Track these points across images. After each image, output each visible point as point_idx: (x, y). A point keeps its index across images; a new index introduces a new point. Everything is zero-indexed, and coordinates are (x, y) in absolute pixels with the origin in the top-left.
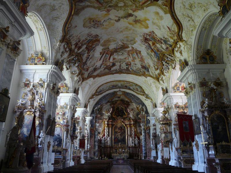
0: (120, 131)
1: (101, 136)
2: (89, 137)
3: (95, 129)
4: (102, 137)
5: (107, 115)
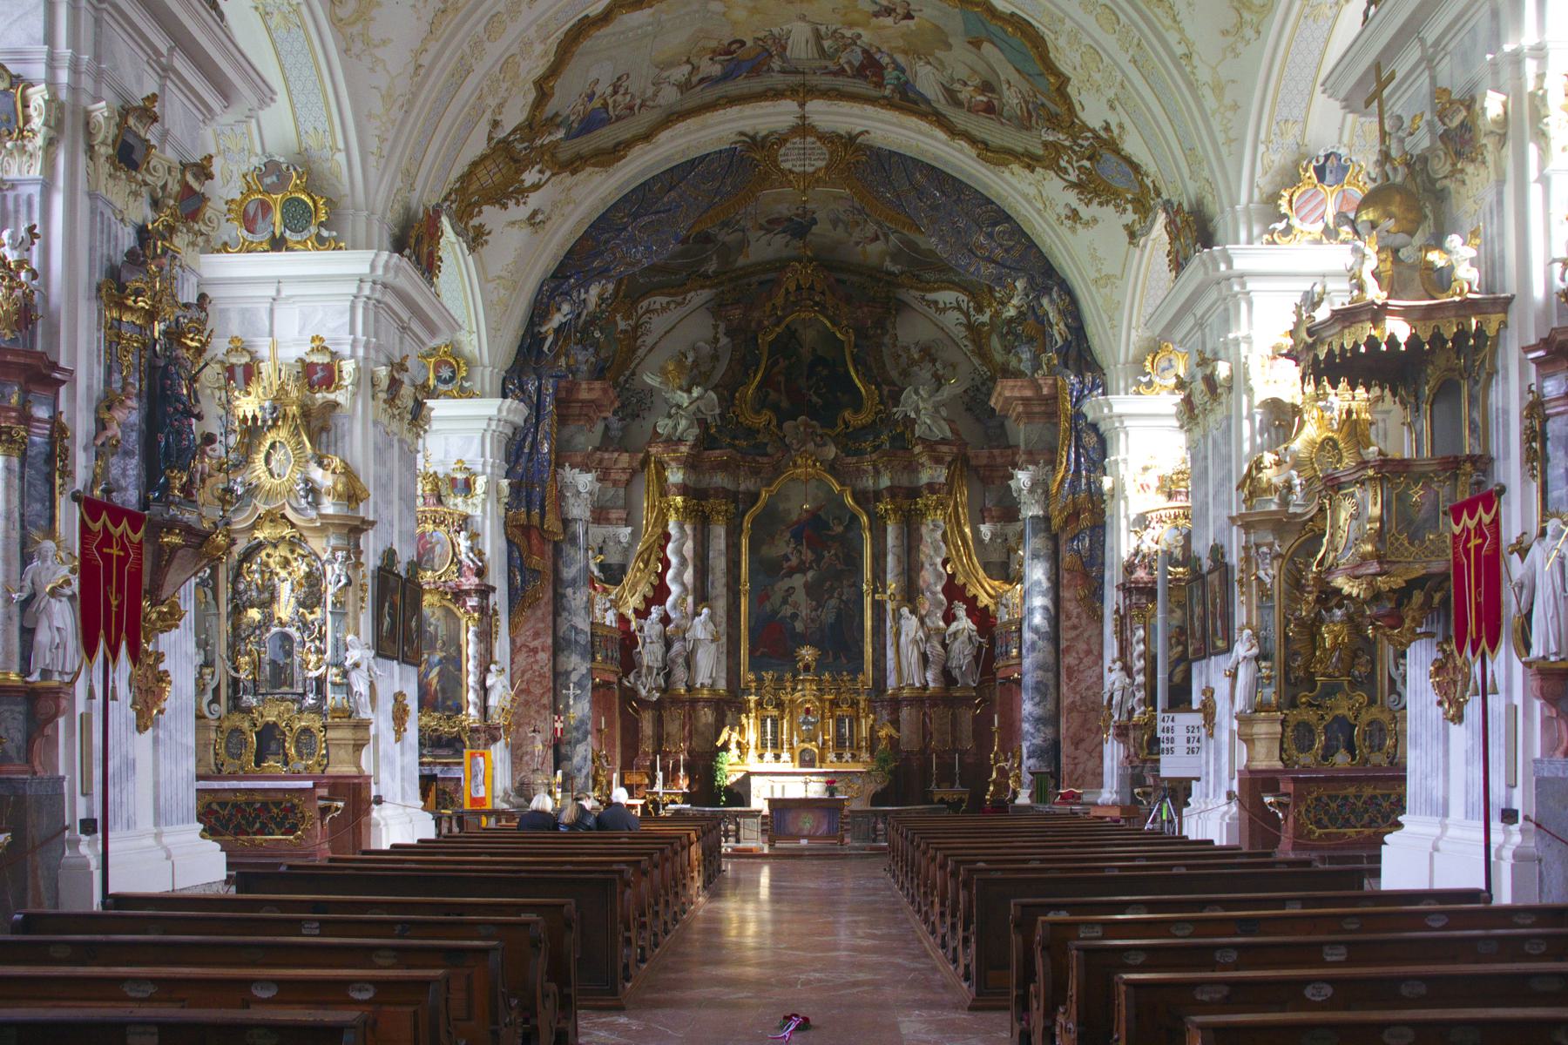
0: (808, 555)
1: (634, 601)
2: (499, 599)
3: (552, 523)
4: (643, 614)
5: (683, 398)
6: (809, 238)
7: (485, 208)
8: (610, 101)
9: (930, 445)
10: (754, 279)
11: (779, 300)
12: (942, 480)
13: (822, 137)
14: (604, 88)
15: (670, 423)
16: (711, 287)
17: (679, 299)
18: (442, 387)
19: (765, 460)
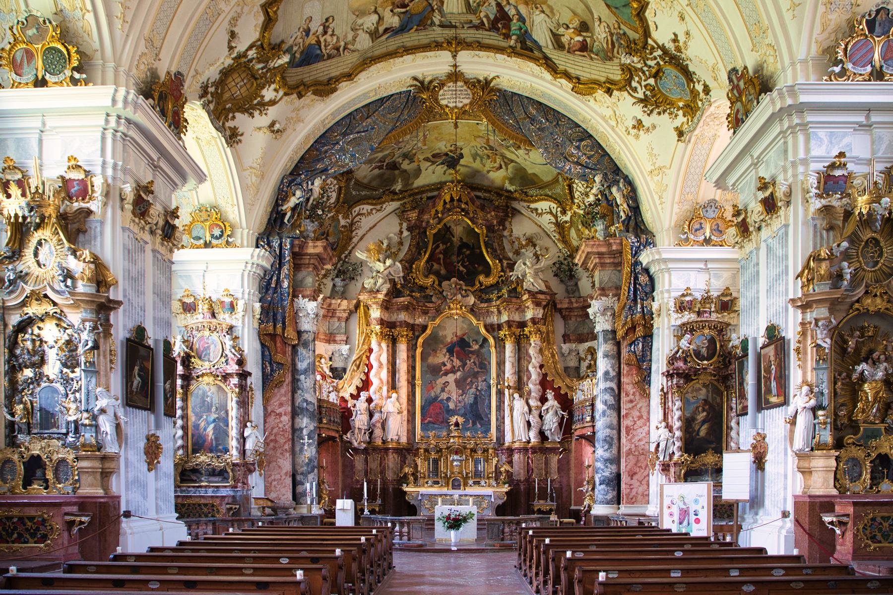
3: (290, 333)
5: (380, 266)
6: (458, 168)
7: (237, 115)
8: (322, 40)
9: (533, 294)
10: (424, 196)
11: (440, 208)
12: (540, 316)
14: (316, 26)
16: (399, 200)
17: (378, 207)
18: (214, 242)
19: (431, 305)
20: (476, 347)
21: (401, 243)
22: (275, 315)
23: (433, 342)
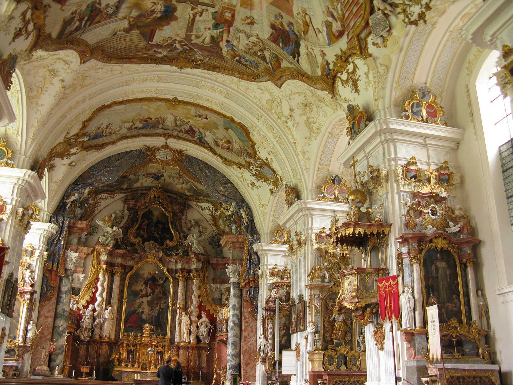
3: (61, 270)
5: (110, 230)
13: (171, 150)
15: (104, 238)
20: (161, 282)
21: (123, 217)
22: (54, 259)
23: (136, 277)
